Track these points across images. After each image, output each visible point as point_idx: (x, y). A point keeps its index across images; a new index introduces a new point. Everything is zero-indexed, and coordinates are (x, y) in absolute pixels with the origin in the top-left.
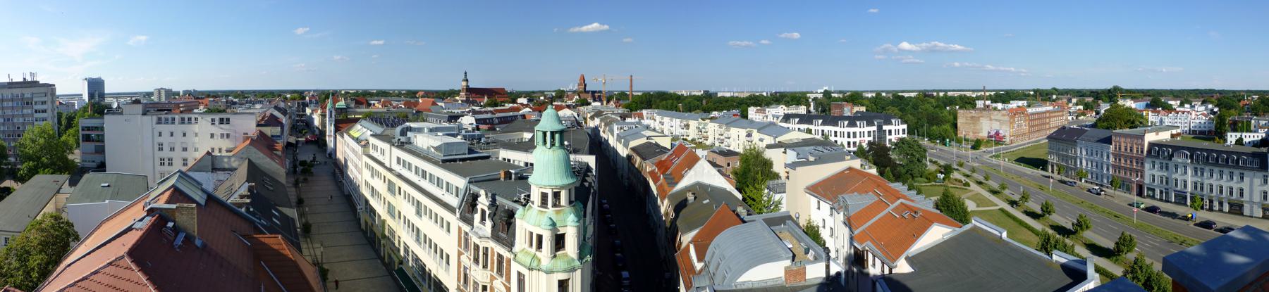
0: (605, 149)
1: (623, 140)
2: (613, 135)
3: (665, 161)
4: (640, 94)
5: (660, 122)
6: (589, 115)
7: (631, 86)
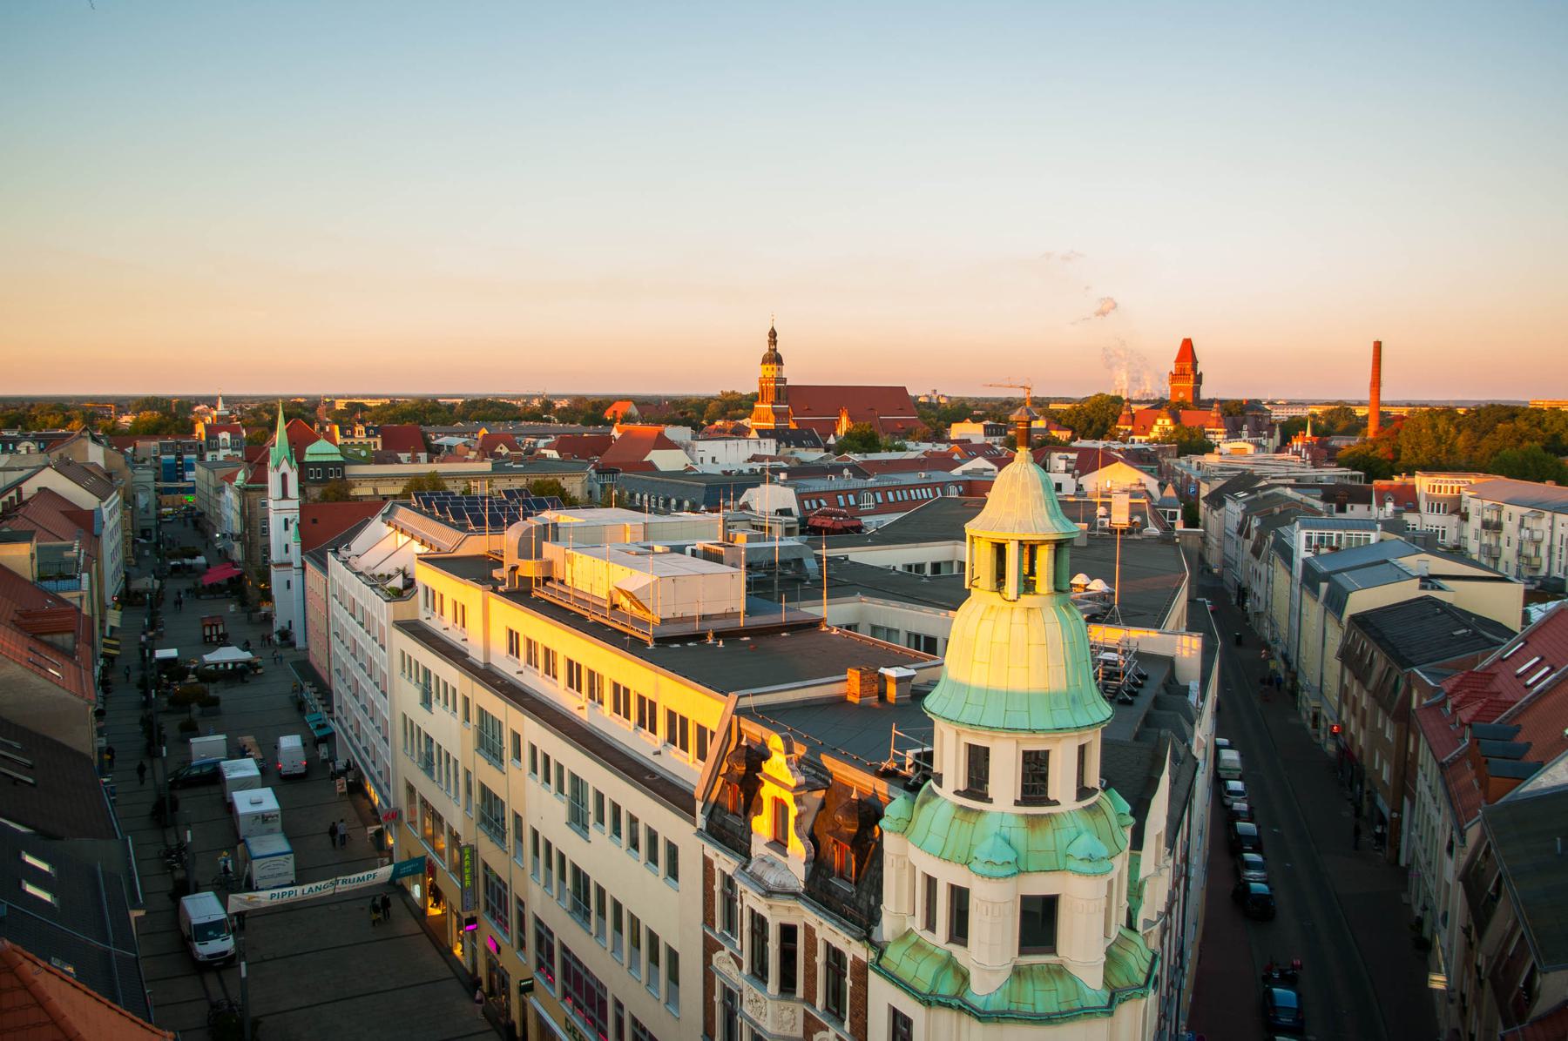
6: (1205, 490)
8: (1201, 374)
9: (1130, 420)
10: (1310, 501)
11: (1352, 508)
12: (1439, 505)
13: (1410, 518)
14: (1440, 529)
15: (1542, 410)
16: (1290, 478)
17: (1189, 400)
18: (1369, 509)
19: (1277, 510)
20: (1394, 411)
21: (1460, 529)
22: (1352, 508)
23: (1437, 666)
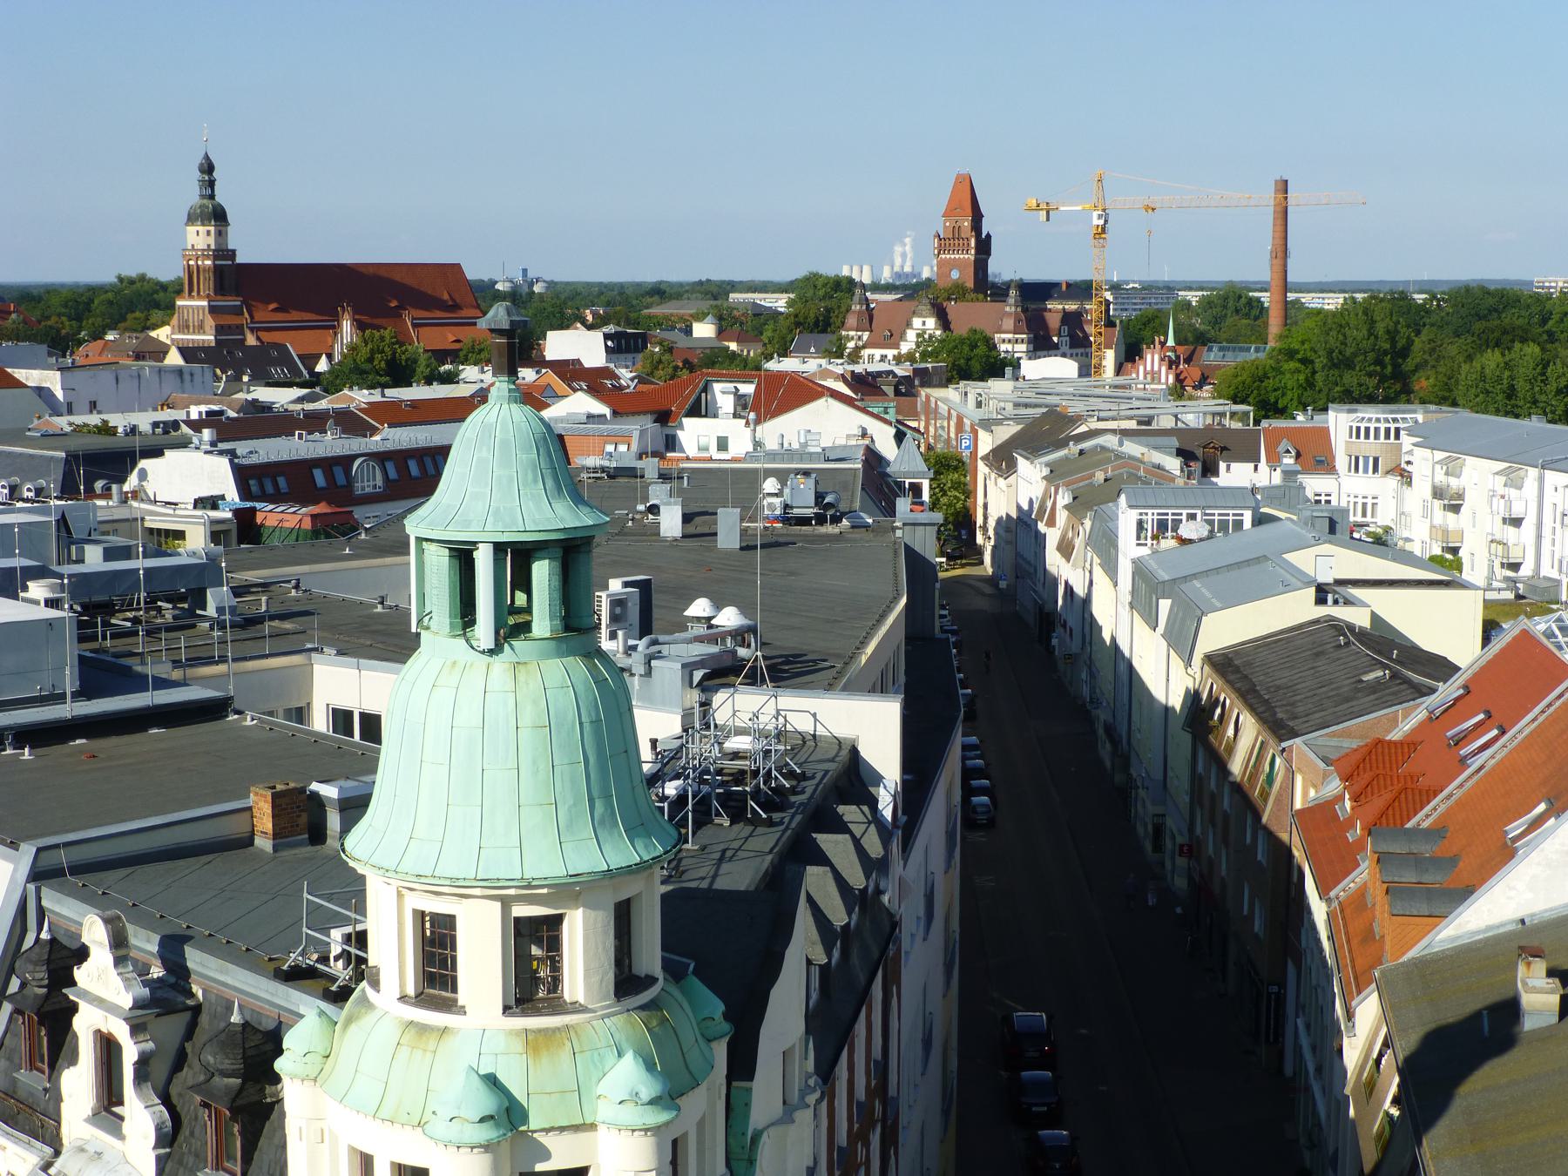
0: (1070, 657)
1: (1165, 605)
2: (1111, 569)
3: (1409, 745)
4: (1333, 302)
5: (1438, 493)
6: (986, 443)
7: (1282, 252)
8: (989, 236)
9: (866, 321)
10: (1158, 457)
12: (1366, 458)
13: (1314, 484)
14: (1370, 501)
15: (1549, 297)
16: (1131, 418)
17: (970, 284)
18: (1256, 468)
19: (1100, 476)
20: (1311, 300)
21: (1399, 499)
23: (1333, 734)
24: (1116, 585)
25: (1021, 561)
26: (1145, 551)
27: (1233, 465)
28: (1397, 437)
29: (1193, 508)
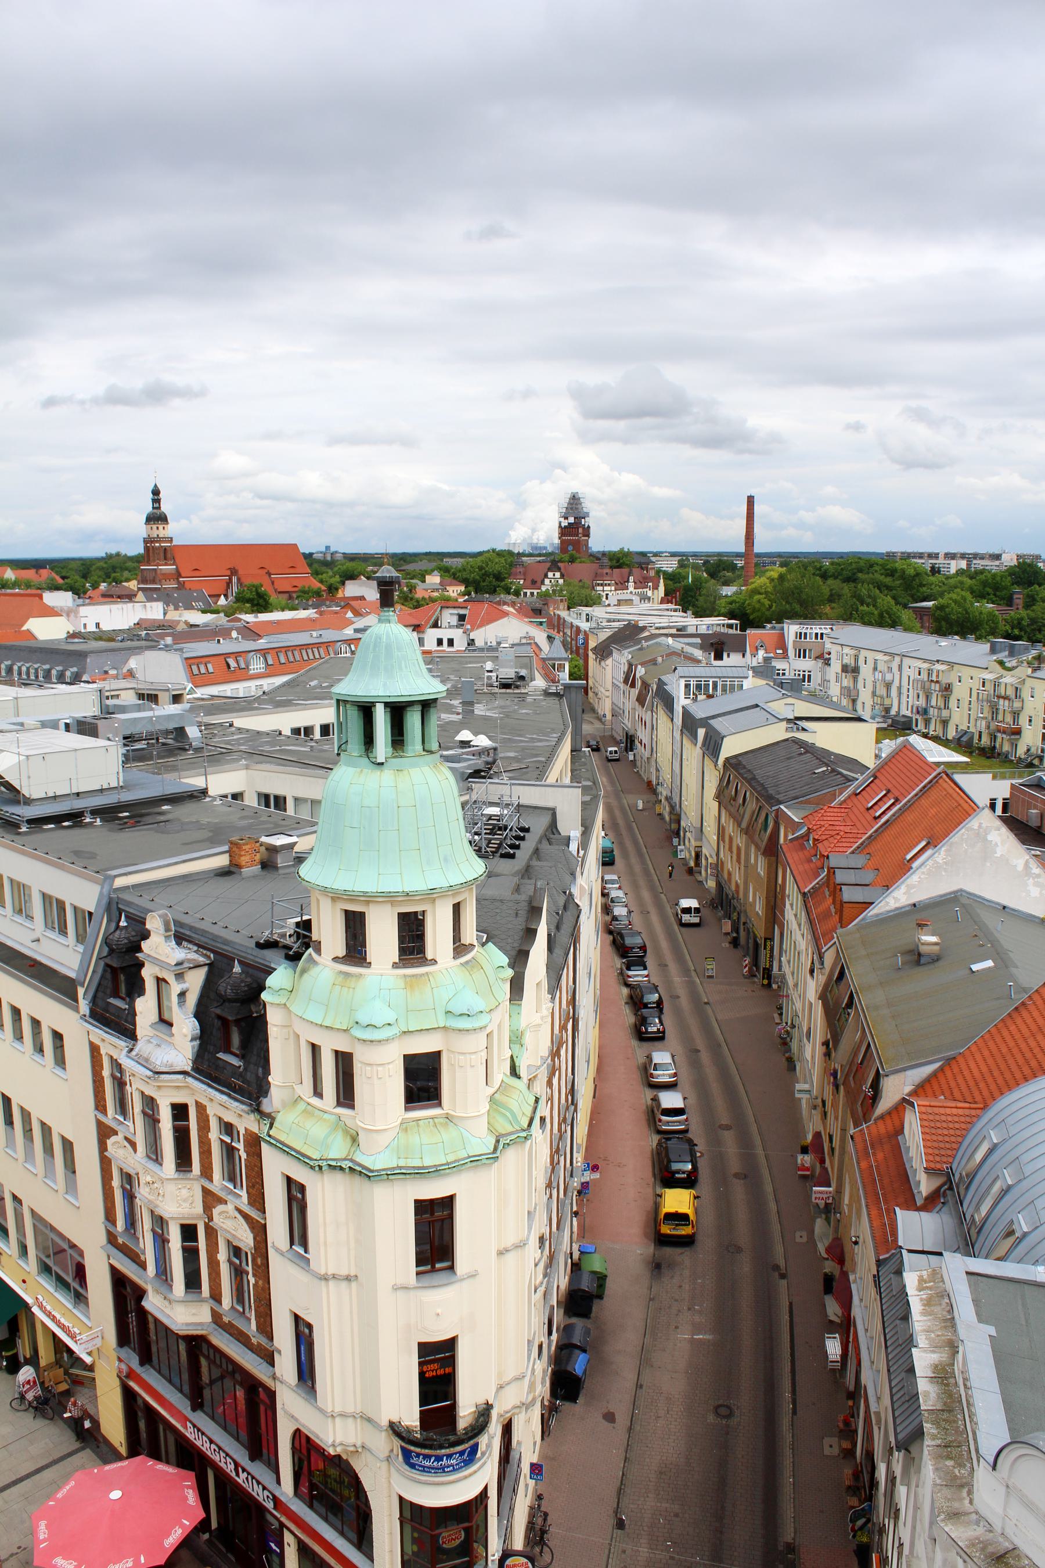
1: (701, 732)
10: (689, 650)
11: (728, 656)
12: (805, 651)
13: (779, 665)
14: (807, 674)
22: (728, 656)
24: (672, 720)
25: (616, 708)
26: (688, 701)
27: (731, 655)
28: (822, 638)
29: (715, 677)
